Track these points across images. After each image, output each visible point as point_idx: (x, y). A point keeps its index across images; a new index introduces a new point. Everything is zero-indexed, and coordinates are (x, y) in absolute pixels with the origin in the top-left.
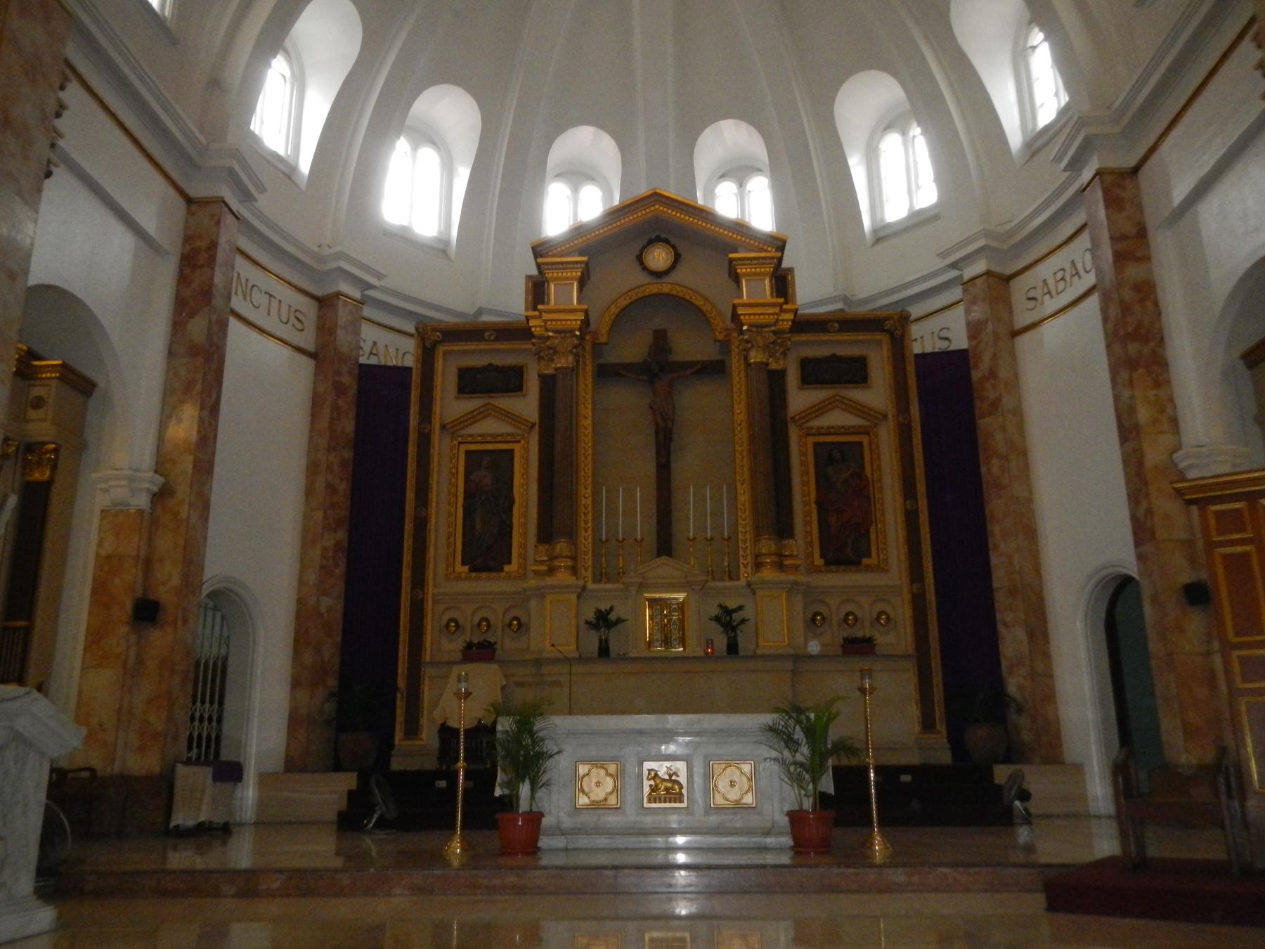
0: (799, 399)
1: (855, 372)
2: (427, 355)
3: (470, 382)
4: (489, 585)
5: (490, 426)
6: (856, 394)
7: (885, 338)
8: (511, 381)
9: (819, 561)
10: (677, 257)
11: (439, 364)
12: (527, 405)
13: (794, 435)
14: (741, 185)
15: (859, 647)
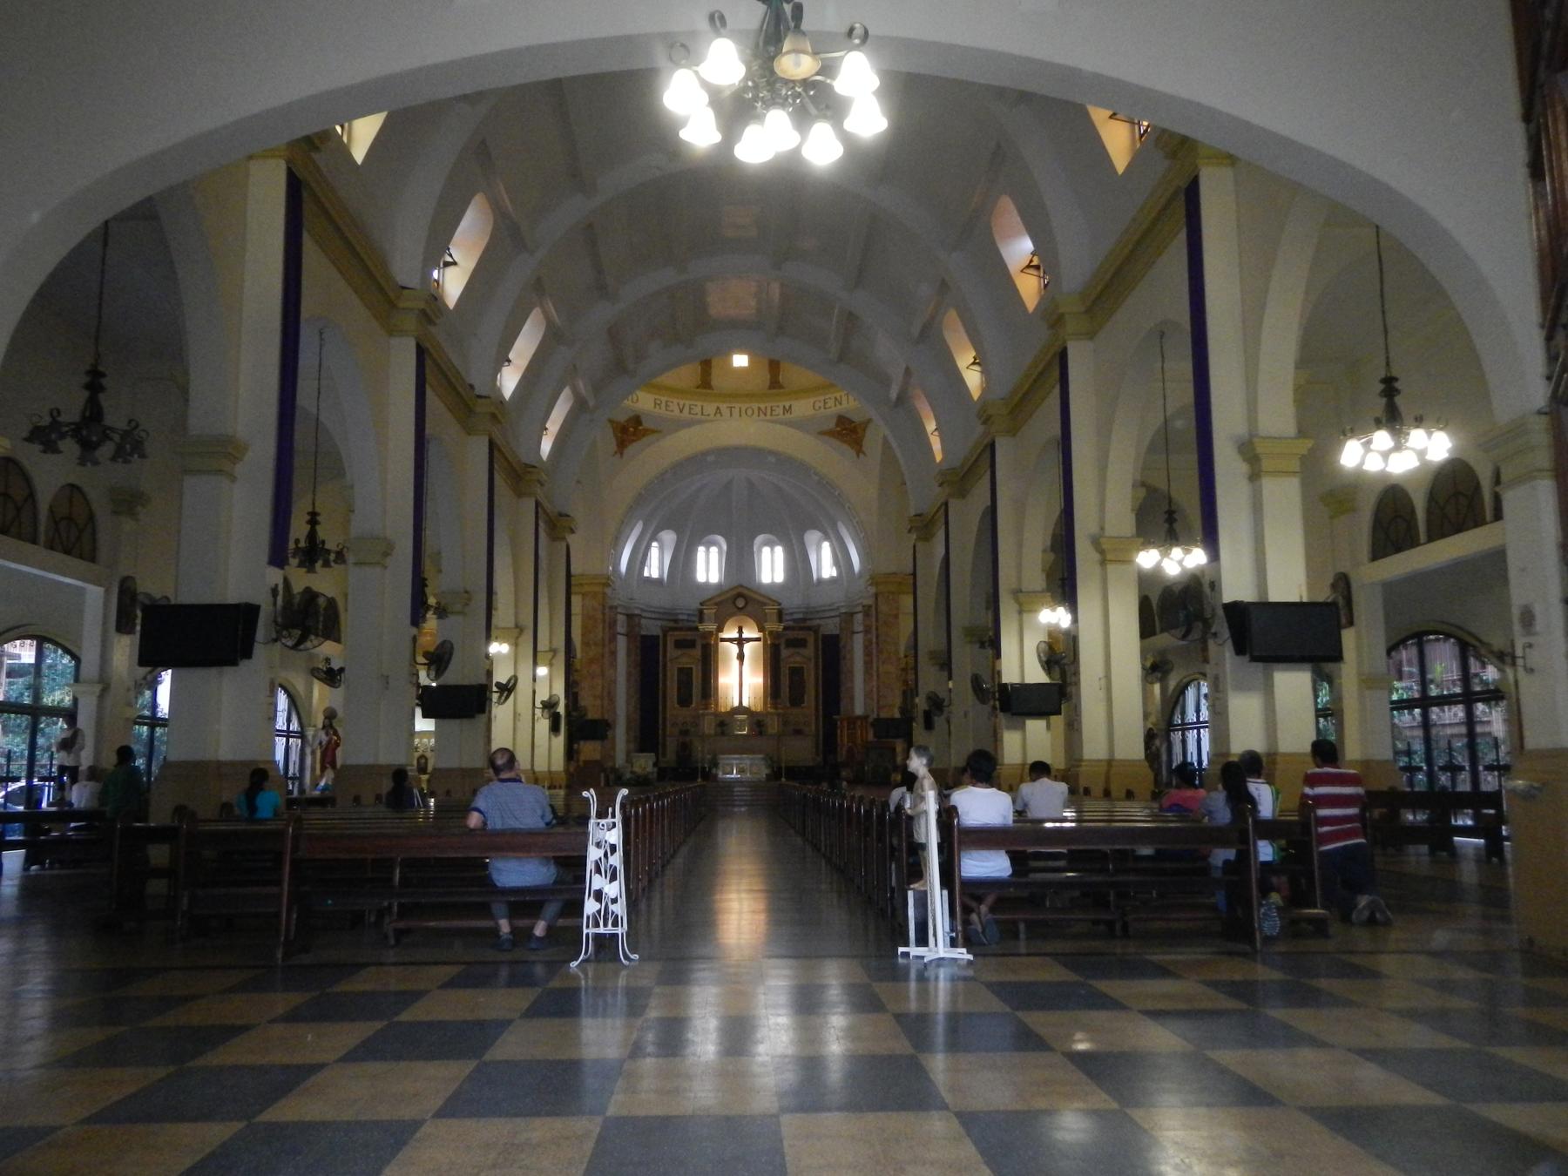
0: (785, 653)
1: (801, 643)
2: (665, 636)
3: (680, 644)
4: (685, 711)
5: (684, 660)
6: (802, 651)
7: (812, 633)
8: (690, 644)
9: (788, 705)
10: (746, 604)
11: (669, 638)
12: (697, 652)
13: (782, 664)
14: (772, 550)
15: (798, 732)
